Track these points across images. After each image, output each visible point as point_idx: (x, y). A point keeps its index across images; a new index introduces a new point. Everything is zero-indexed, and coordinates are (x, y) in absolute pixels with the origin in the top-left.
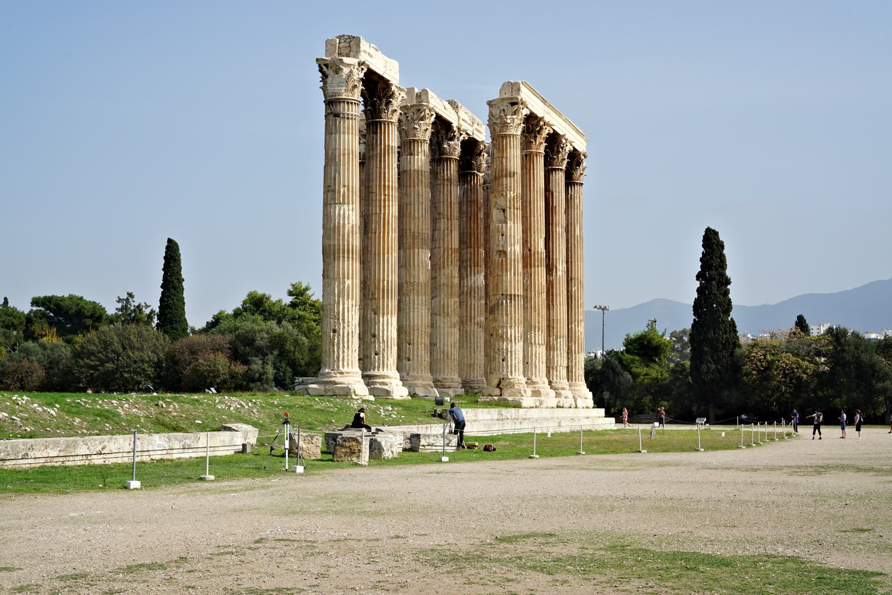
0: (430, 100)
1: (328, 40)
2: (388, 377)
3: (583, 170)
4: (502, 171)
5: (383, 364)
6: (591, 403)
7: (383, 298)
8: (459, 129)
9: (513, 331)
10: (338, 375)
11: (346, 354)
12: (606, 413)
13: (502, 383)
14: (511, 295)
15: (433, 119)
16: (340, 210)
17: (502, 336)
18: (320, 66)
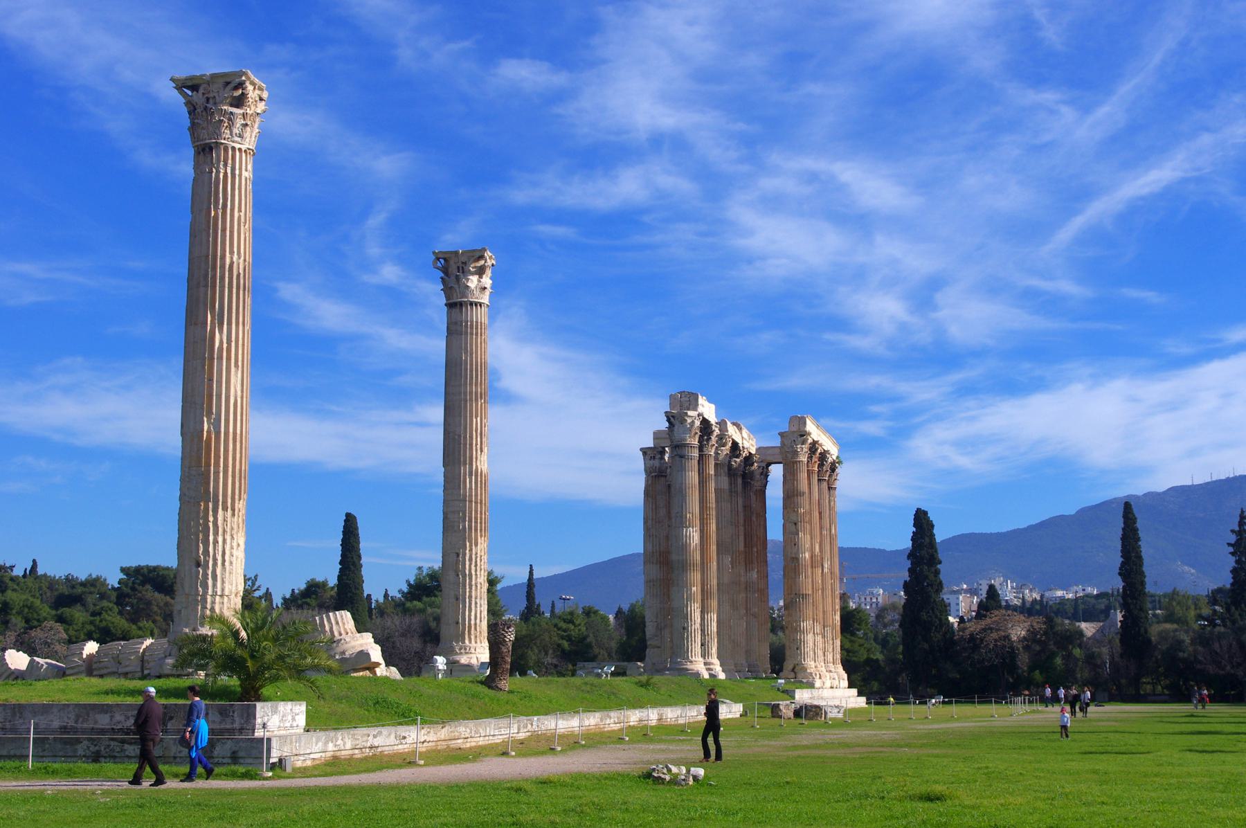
0: (729, 429)
1: (672, 395)
2: (713, 664)
3: (837, 475)
4: (793, 492)
5: (708, 653)
6: (845, 683)
7: (707, 599)
8: (743, 447)
9: (805, 624)
10: (689, 663)
11: (693, 646)
12: (858, 692)
13: (797, 668)
14: (806, 595)
15: (730, 444)
16: (687, 530)
17: (796, 629)
18: (667, 417)
